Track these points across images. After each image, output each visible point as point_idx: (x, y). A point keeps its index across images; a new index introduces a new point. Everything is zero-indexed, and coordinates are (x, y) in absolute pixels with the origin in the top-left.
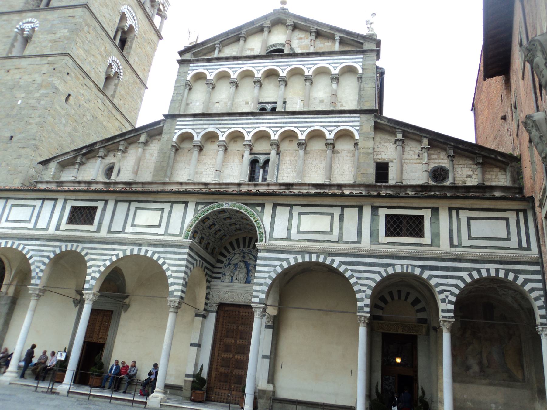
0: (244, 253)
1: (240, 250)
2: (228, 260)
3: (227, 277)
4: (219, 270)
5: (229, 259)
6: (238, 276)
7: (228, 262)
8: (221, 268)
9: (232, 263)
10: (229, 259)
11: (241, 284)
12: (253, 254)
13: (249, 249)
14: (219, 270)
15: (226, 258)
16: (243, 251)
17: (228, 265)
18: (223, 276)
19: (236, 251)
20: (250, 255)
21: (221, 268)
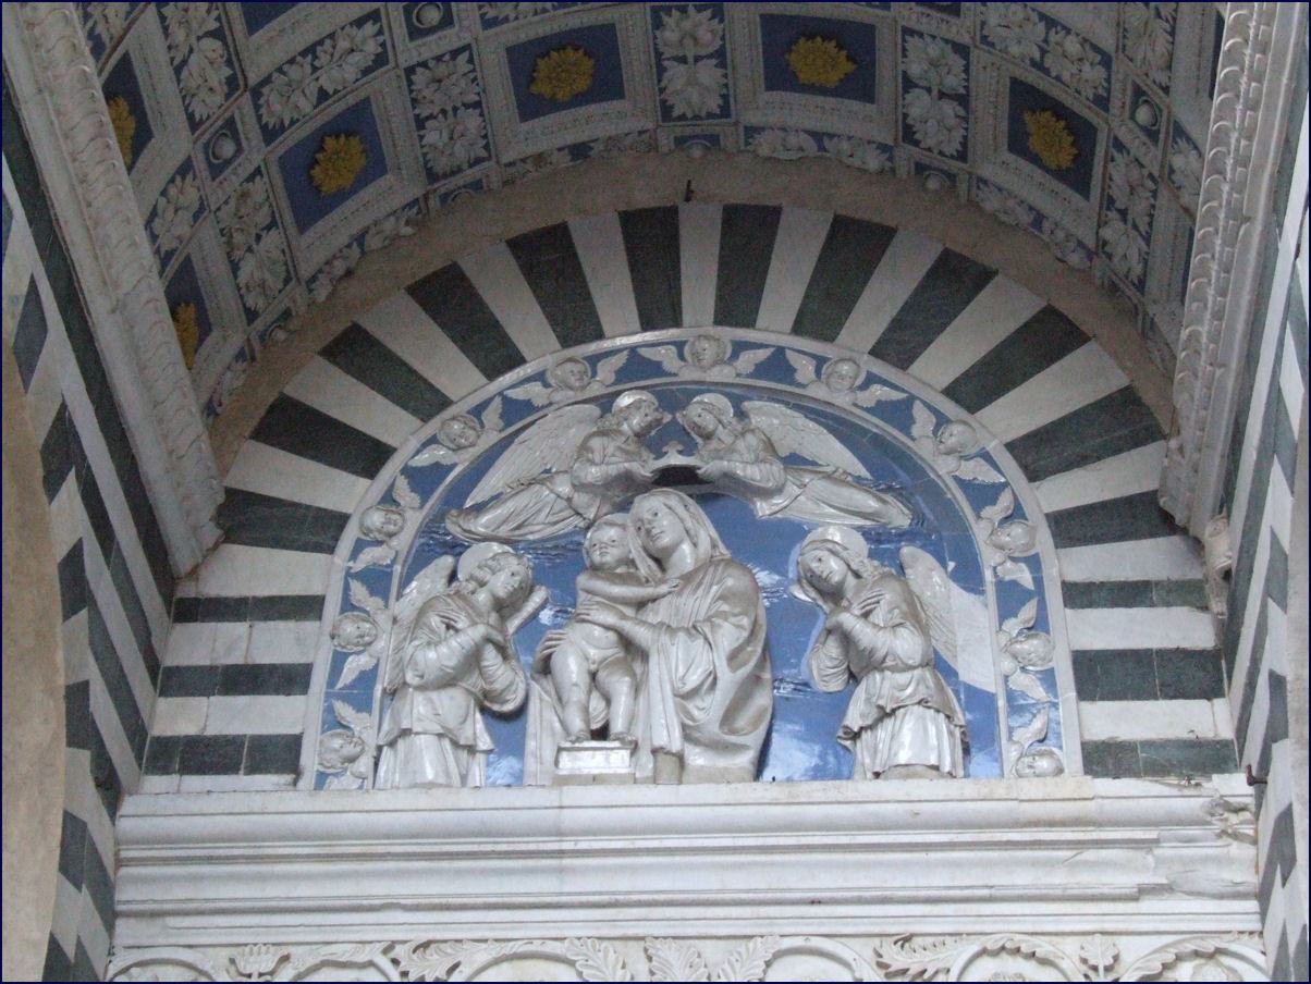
0: (673, 398)
1: (606, 371)
2: (406, 495)
3: (419, 709)
4: (274, 643)
5: (423, 479)
6: (621, 686)
7: (414, 519)
8: (306, 607)
9: (481, 525)
10: (423, 479)
11: (686, 792)
12: (819, 392)
13: (740, 347)
14: (274, 643)
15: (370, 472)
16: (656, 369)
17: (419, 560)
18: (345, 711)
19: (540, 377)
20: (769, 417)
21: (306, 607)
